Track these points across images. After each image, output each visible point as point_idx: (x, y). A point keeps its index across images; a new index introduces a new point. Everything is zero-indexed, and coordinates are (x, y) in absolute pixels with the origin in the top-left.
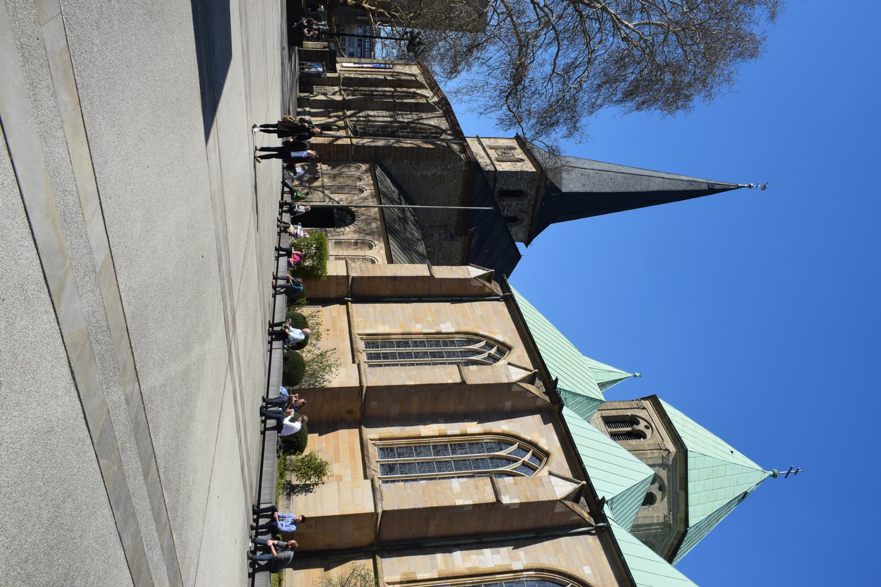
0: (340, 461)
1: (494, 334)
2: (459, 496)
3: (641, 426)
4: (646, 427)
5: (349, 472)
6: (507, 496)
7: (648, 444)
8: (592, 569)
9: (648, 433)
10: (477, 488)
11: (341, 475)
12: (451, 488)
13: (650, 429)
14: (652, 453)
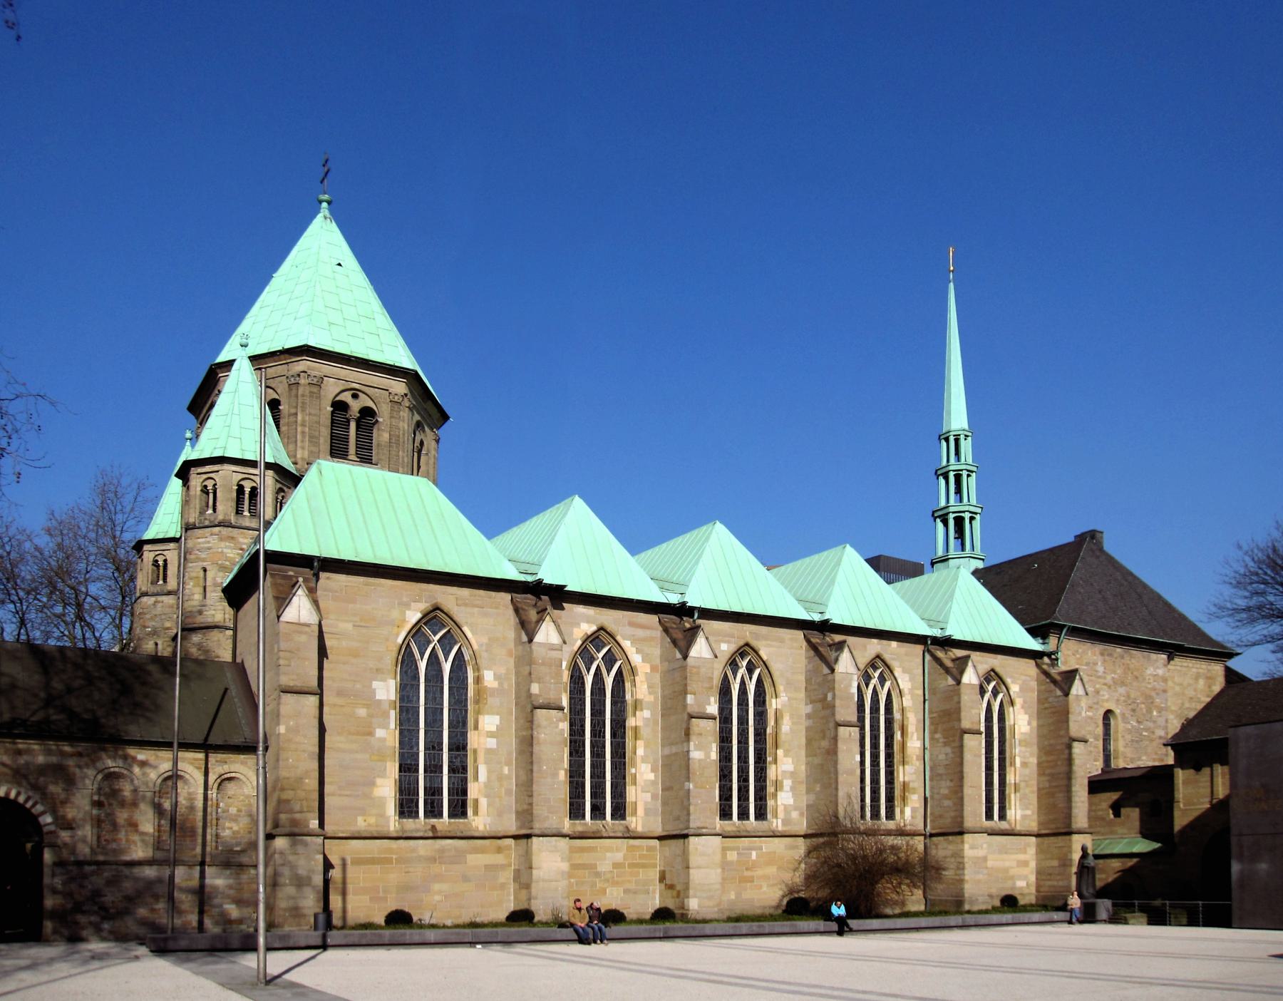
0: (596, 865)
2: (708, 755)
3: (355, 406)
4: (355, 396)
5: (608, 855)
6: (707, 707)
7: (391, 417)
8: (725, 642)
9: (365, 401)
10: (701, 734)
11: (613, 864)
12: (700, 760)
13: (360, 394)
14: (403, 421)
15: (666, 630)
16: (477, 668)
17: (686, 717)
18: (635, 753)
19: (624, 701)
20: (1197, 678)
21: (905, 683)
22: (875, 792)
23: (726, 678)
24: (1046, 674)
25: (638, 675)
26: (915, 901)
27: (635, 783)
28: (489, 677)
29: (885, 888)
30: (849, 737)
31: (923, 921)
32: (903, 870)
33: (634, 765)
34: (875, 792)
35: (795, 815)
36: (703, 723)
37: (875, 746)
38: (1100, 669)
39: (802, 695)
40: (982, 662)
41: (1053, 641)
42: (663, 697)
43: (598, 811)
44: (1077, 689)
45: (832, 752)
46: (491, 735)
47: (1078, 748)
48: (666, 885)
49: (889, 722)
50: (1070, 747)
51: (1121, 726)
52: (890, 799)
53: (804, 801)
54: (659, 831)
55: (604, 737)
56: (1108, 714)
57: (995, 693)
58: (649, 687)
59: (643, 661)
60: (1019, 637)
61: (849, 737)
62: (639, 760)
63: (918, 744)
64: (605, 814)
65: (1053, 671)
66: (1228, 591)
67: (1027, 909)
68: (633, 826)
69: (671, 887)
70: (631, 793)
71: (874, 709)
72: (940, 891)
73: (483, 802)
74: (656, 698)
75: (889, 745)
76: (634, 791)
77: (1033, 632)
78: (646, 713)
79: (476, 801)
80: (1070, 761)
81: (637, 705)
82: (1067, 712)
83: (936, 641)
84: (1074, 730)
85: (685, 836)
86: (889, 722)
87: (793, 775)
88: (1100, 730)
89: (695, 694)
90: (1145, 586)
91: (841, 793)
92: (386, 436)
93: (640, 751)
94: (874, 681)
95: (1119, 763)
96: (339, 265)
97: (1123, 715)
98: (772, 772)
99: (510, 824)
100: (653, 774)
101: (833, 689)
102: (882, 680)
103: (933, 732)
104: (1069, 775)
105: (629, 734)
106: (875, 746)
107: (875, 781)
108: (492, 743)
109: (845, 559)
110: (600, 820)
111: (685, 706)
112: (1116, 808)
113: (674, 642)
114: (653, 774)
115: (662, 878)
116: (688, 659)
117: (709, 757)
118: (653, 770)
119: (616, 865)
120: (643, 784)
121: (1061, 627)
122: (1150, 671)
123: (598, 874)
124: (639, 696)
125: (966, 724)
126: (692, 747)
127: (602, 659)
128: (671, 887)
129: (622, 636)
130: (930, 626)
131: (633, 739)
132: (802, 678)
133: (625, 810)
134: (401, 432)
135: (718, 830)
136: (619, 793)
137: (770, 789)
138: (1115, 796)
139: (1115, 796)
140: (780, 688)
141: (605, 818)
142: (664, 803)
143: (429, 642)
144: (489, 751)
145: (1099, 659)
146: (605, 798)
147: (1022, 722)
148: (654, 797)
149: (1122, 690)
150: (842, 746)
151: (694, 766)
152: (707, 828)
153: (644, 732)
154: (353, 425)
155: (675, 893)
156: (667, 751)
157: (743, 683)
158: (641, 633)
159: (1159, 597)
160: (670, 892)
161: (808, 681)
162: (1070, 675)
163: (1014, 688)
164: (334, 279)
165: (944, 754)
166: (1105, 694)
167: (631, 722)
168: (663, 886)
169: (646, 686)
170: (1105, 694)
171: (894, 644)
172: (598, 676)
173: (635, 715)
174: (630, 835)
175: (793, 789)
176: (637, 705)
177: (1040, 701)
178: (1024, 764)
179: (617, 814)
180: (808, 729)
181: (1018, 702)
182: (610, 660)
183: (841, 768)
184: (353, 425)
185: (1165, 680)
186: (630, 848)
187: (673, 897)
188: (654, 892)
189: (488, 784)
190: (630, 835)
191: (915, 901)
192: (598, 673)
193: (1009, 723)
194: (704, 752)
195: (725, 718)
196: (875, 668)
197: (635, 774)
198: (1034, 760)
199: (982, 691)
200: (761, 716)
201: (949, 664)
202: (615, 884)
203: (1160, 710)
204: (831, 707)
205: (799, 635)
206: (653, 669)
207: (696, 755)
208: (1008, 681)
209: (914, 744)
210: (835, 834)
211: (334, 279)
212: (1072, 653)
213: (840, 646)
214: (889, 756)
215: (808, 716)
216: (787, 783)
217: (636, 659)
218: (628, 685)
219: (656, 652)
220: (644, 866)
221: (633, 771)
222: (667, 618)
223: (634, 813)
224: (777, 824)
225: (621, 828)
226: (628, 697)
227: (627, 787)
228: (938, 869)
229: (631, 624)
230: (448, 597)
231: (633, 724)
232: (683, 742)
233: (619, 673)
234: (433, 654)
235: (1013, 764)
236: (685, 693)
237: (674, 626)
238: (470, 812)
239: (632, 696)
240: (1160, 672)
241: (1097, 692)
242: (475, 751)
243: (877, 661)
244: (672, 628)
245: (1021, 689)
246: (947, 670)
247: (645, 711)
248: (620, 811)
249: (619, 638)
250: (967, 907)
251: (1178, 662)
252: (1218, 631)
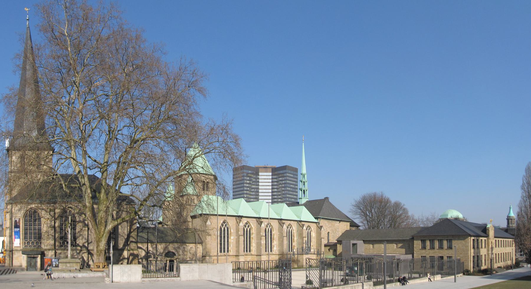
15: (257, 221)
16: (230, 229)
20: (345, 225)
21: (294, 228)
22: (289, 247)
23: (266, 229)
24: (318, 226)
26: (296, 266)
28: (232, 231)
29: (290, 264)
30: (285, 238)
31: (297, 269)
32: (294, 261)
33: (252, 243)
34: (289, 247)
35: (277, 251)
37: (289, 239)
38: (327, 225)
39: (277, 231)
40: (306, 224)
41: (319, 220)
42: (257, 232)
43: (247, 251)
44: (322, 229)
45: (283, 241)
46: (232, 240)
47: (322, 240)
49: (291, 235)
50: (321, 239)
51: (331, 235)
52: (292, 248)
53: (278, 249)
54: (256, 254)
56: (328, 233)
57: (309, 229)
60: (312, 219)
61: (285, 238)
63: (296, 239)
65: (319, 226)
66: (351, 207)
67: (313, 267)
71: (289, 233)
72: (300, 264)
73: (231, 250)
75: (291, 239)
77: (315, 218)
78: (254, 235)
79: (230, 250)
80: (321, 242)
82: (321, 233)
83: (299, 221)
84: (322, 236)
85: (261, 256)
86: (291, 235)
87: (276, 244)
88: (327, 235)
90: (336, 208)
91: (284, 248)
93: (253, 241)
94: (289, 228)
95: (330, 241)
97: (331, 233)
98: (273, 244)
99: (235, 254)
101: (283, 231)
102: (290, 228)
103: (298, 237)
104: (321, 244)
105: (251, 238)
106: (289, 239)
107: (289, 245)
108: (232, 241)
109: (284, 206)
111: (260, 234)
112: (329, 250)
118: (255, 244)
121: (320, 218)
122: (336, 225)
125: (304, 236)
130: (298, 218)
132: (278, 228)
137: (273, 247)
138: (329, 248)
139: (329, 248)
140: (274, 230)
142: (257, 250)
143: (223, 225)
144: (232, 242)
145: (327, 223)
147: (313, 234)
149: (331, 228)
150: (284, 240)
151: (262, 244)
153: (254, 238)
156: (257, 241)
157: (268, 229)
158: (253, 222)
159: (339, 210)
161: (278, 229)
162: (321, 227)
163: (312, 229)
165: (300, 241)
166: (328, 229)
167: (252, 236)
170: (328, 229)
171: (292, 222)
172: (247, 229)
174: (252, 255)
175: (276, 247)
177: (317, 231)
178: (314, 242)
180: (278, 237)
181: (313, 231)
182: (248, 226)
183: (284, 244)
185: (339, 226)
186: (252, 257)
189: (232, 248)
190: (252, 255)
191: (296, 266)
192: (247, 229)
193: (311, 234)
194: (263, 242)
195: (266, 235)
196: (289, 225)
198: (315, 241)
199: (307, 229)
200: (271, 235)
201: (301, 225)
203: (338, 232)
204: (282, 234)
205: (277, 221)
206: (255, 227)
208: (311, 227)
209: (295, 239)
210: (283, 255)
212: (322, 222)
213: (284, 223)
214: (291, 241)
215: (279, 235)
216: (275, 246)
217: (252, 226)
218: (251, 230)
219: (255, 225)
222: (257, 219)
224: (274, 253)
228: (299, 261)
229: (252, 220)
230: (225, 218)
233: (250, 228)
234: (224, 227)
235: (312, 242)
236: (260, 232)
238: (229, 252)
240: (338, 225)
241: (327, 229)
242: (230, 242)
243: (290, 225)
245: (314, 229)
246: (301, 226)
248: (250, 251)
250: (304, 267)
251: (341, 222)
252: (350, 215)
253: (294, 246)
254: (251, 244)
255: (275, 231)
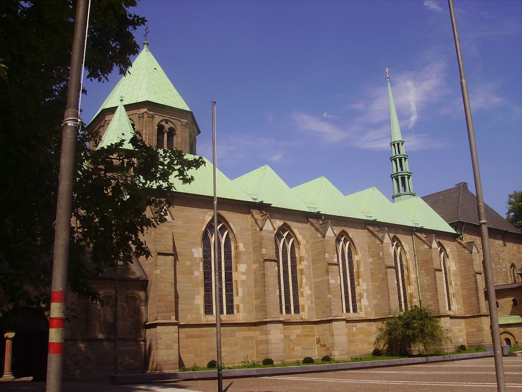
1: (204, 220)
3: (167, 126)
4: (167, 123)
5: (294, 331)
7: (182, 132)
9: (170, 125)
14: (187, 134)
17: (325, 264)
18: (302, 282)
19: (295, 257)
25: (301, 245)
27: (302, 296)
33: (301, 287)
36: (333, 267)
48: (321, 344)
55: (288, 274)
58: (306, 251)
59: (303, 238)
62: (304, 285)
64: (291, 311)
68: (303, 317)
69: (324, 346)
70: (302, 301)
74: (309, 256)
76: (303, 299)
78: (305, 263)
81: (301, 259)
89: (329, 253)
92: (180, 140)
93: (304, 281)
96: (155, 69)
100: (310, 291)
110: (289, 314)
113: (317, 229)
114: (310, 291)
115: (318, 341)
116: (326, 238)
117: (337, 283)
118: (311, 289)
119: (298, 336)
120: (306, 296)
123: (291, 341)
124: (302, 255)
126: (330, 279)
127: (285, 237)
128: (324, 346)
129: (293, 227)
131: (301, 275)
133: (299, 309)
134: (186, 138)
135: (344, 317)
136: (296, 301)
141: (291, 313)
142: (317, 305)
146: (290, 303)
148: (312, 302)
152: (339, 316)
153: (306, 272)
154: (166, 135)
155: (326, 349)
156: (316, 280)
160: (323, 348)
164: (154, 74)
167: (299, 267)
168: (319, 345)
169: (305, 250)
173: (300, 263)
176: (301, 259)
179: (296, 311)
184: (166, 135)
187: (325, 351)
188: (315, 348)
197: (303, 292)
202: (298, 345)
206: (307, 242)
207: (332, 281)
211: (154, 74)
217: (300, 237)
218: (296, 250)
220: (309, 336)
221: (302, 290)
223: (303, 311)
225: (299, 318)
226: (297, 255)
227: (299, 298)
231: (301, 268)
232: (325, 276)
237: (316, 222)
239: (299, 254)
244: (315, 223)
247: (305, 261)
249: (292, 228)
253: (411, 295)
254: (300, 290)
255: (360, 255)
